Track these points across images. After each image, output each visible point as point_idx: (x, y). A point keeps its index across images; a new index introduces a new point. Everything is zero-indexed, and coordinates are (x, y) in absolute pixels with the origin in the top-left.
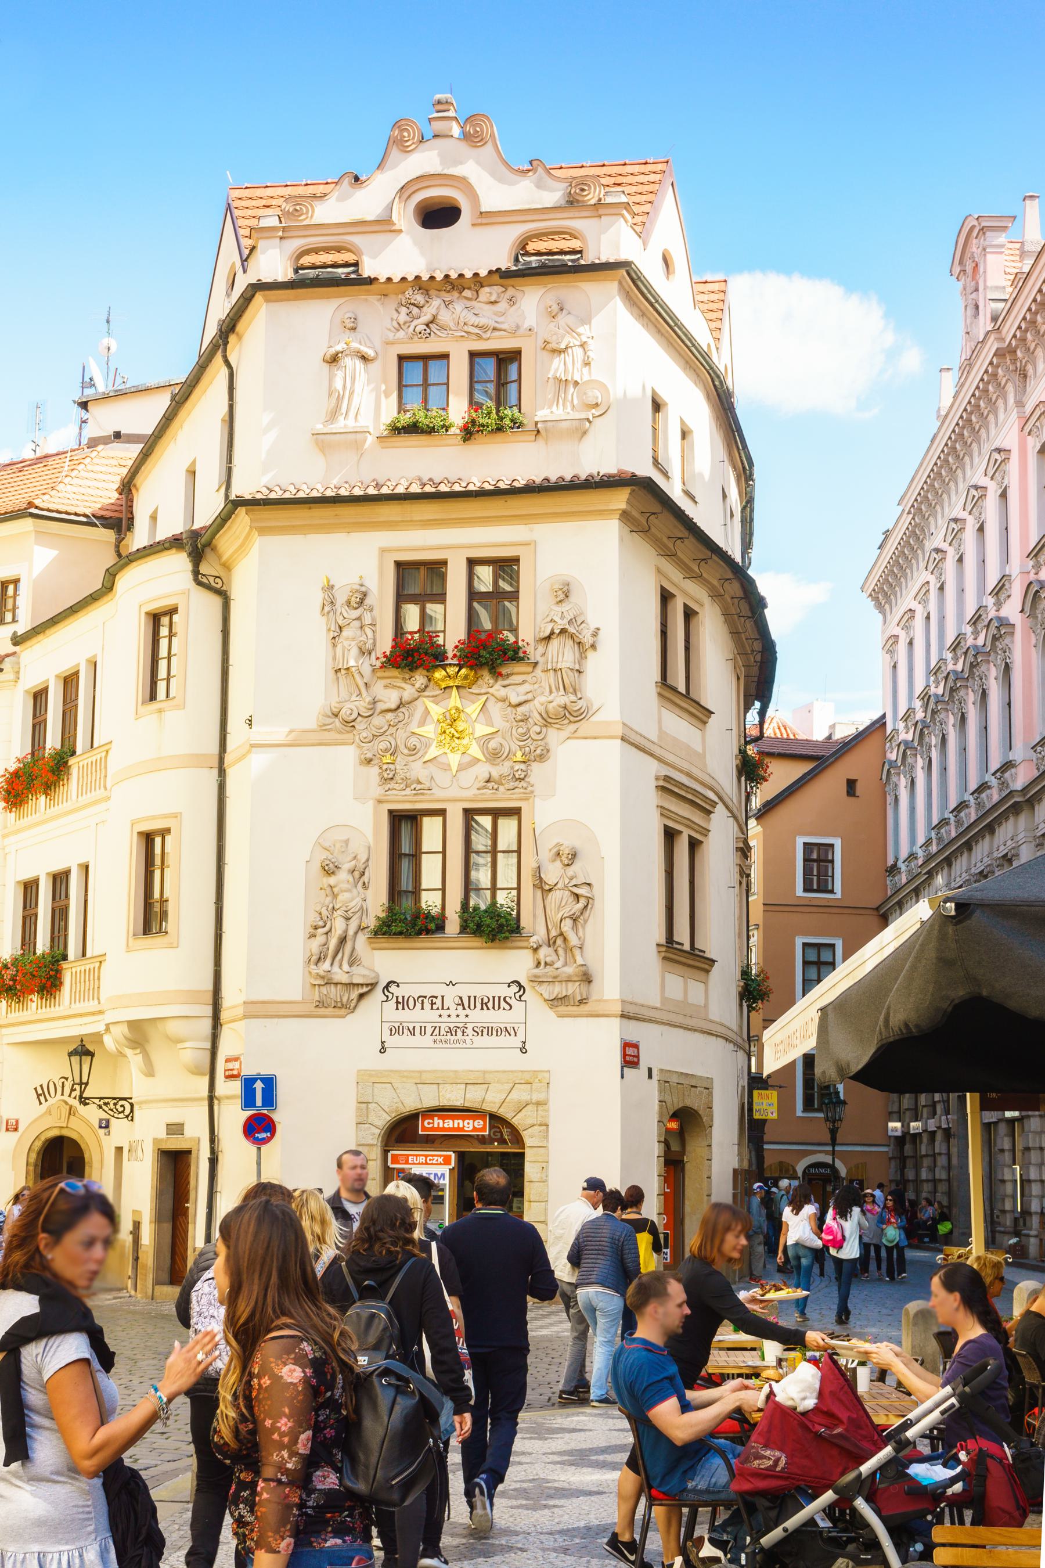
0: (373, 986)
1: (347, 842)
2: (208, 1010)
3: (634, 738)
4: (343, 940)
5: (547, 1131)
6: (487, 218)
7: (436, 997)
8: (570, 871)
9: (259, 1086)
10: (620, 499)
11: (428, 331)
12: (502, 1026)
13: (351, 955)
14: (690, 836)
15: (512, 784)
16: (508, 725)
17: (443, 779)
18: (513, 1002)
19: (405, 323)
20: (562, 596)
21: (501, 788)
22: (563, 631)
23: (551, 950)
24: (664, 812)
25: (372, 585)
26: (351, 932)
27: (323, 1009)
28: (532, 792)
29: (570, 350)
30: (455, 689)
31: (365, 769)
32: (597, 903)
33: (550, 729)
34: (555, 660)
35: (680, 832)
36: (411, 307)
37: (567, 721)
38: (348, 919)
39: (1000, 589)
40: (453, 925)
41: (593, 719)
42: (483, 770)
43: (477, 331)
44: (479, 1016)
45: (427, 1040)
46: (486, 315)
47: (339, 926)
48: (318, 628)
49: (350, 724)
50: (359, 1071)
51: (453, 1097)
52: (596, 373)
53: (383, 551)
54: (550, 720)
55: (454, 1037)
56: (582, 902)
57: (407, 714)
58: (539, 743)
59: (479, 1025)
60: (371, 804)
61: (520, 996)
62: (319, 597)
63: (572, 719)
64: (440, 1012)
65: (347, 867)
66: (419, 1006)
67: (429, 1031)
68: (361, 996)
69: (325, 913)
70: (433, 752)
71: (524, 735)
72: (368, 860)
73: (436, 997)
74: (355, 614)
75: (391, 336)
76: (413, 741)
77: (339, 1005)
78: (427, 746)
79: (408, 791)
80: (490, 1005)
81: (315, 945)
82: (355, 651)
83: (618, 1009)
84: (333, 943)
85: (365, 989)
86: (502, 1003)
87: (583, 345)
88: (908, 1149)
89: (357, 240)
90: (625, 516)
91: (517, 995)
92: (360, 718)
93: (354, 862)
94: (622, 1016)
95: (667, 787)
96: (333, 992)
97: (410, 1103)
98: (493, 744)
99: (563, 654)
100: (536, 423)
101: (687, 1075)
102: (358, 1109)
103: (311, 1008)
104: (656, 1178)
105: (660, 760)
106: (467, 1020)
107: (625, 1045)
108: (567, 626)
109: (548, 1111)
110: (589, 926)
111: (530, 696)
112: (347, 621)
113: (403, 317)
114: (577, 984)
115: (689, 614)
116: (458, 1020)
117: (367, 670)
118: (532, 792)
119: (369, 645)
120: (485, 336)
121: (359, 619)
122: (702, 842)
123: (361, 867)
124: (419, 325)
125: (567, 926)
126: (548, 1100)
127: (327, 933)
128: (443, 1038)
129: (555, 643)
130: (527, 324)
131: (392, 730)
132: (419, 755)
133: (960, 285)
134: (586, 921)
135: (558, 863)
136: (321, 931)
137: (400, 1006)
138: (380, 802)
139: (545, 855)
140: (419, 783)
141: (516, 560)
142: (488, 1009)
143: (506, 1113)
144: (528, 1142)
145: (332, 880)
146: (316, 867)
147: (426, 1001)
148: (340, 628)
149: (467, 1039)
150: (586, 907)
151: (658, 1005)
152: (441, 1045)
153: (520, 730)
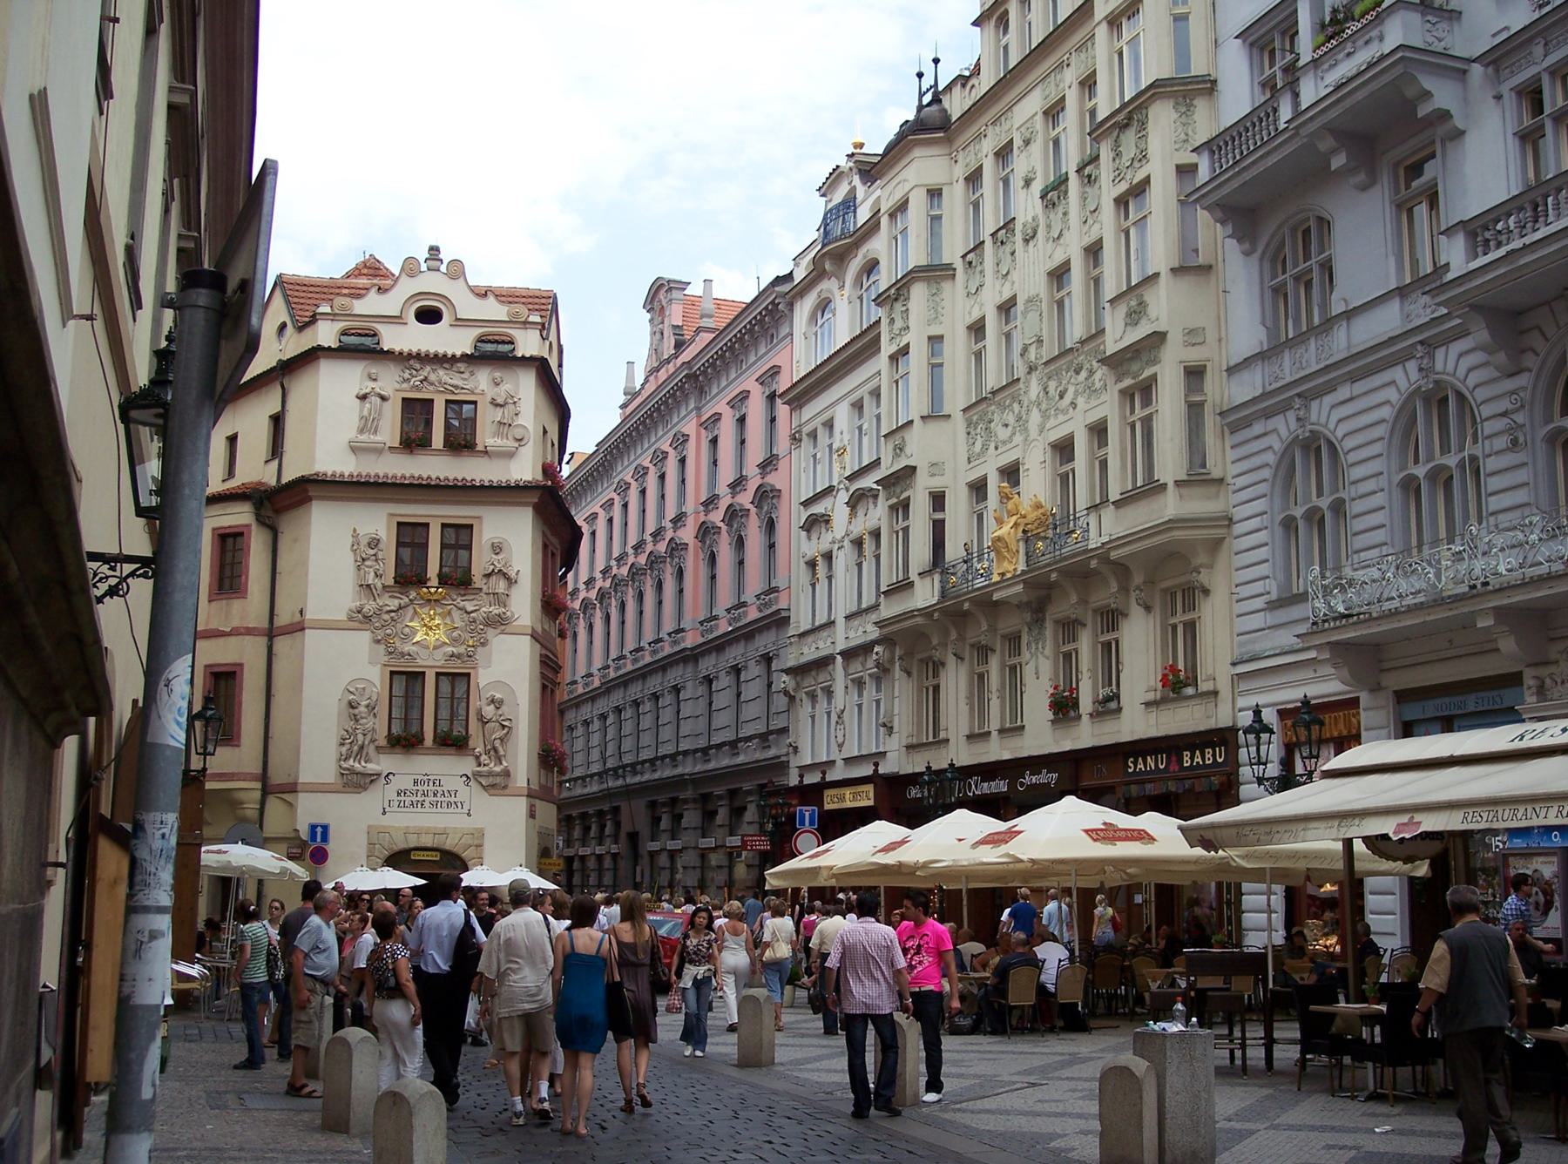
2: (258, 785)
4: (362, 747)
6: (460, 322)
8: (500, 712)
17: (424, 653)
22: (500, 571)
24: (543, 676)
25: (383, 535)
31: (377, 646)
39: (679, 520)
42: (450, 649)
48: (349, 560)
51: (427, 841)
52: (520, 420)
62: (350, 540)
65: (364, 703)
68: (372, 781)
70: (417, 638)
74: (372, 552)
76: (407, 630)
81: (344, 750)
82: (372, 574)
84: (356, 748)
88: (576, 865)
94: (529, 796)
97: (402, 845)
98: (455, 634)
115: (553, 554)
117: (379, 586)
123: (372, 704)
124: (415, 381)
129: (494, 578)
130: (481, 388)
133: (648, 316)
139: (484, 701)
141: (471, 527)
145: (356, 711)
146: (345, 702)
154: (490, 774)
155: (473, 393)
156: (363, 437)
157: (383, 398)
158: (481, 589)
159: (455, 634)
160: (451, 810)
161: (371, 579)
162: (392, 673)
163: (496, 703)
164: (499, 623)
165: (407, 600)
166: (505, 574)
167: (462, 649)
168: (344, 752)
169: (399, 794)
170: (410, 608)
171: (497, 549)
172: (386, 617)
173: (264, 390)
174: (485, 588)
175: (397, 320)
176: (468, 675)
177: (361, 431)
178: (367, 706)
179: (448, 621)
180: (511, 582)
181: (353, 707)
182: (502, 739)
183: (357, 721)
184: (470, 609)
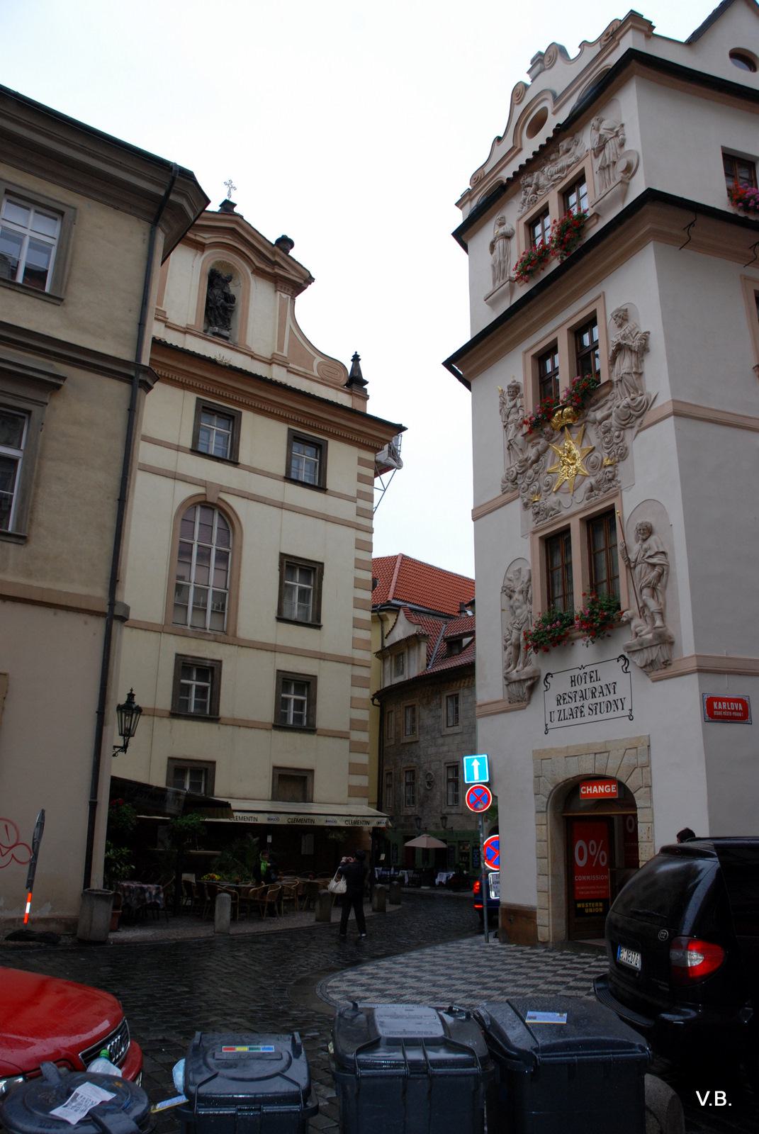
1: (519, 571)
3: (701, 413)
5: (651, 792)
8: (645, 546)
10: (647, 223)
16: (599, 440)
17: (566, 500)
19: (525, 200)
20: (620, 321)
21: (601, 493)
25: (520, 379)
27: (514, 704)
28: (620, 487)
29: (607, 144)
30: (566, 428)
32: (671, 569)
37: (634, 418)
41: (652, 408)
43: (558, 175)
46: (564, 161)
51: (587, 766)
53: (525, 352)
54: (624, 423)
56: (657, 569)
57: (543, 460)
61: (626, 668)
62: (498, 400)
63: (637, 413)
68: (532, 689)
71: (608, 443)
72: (530, 580)
76: (548, 478)
77: (519, 699)
78: (555, 480)
79: (549, 519)
83: (693, 665)
85: (529, 683)
90: (660, 236)
91: (624, 668)
92: (519, 476)
94: (700, 671)
96: (514, 687)
103: (506, 704)
111: (610, 411)
113: (523, 196)
114: (659, 646)
117: (519, 437)
118: (620, 487)
120: (563, 175)
121: (515, 406)
123: (524, 586)
126: (649, 761)
134: (665, 587)
135: (640, 542)
140: (554, 509)
144: (639, 803)
150: (660, 575)
153: (607, 440)
156: (497, 285)
158: (610, 383)
159: (592, 459)
160: (611, 714)
163: (646, 532)
164: (636, 415)
166: (630, 349)
167: (600, 475)
169: (559, 703)
170: (550, 452)
171: (622, 317)
173: (264, 280)
174: (615, 379)
175: (515, 150)
178: (522, 592)
179: (585, 446)
181: (510, 597)
182: (654, 589)
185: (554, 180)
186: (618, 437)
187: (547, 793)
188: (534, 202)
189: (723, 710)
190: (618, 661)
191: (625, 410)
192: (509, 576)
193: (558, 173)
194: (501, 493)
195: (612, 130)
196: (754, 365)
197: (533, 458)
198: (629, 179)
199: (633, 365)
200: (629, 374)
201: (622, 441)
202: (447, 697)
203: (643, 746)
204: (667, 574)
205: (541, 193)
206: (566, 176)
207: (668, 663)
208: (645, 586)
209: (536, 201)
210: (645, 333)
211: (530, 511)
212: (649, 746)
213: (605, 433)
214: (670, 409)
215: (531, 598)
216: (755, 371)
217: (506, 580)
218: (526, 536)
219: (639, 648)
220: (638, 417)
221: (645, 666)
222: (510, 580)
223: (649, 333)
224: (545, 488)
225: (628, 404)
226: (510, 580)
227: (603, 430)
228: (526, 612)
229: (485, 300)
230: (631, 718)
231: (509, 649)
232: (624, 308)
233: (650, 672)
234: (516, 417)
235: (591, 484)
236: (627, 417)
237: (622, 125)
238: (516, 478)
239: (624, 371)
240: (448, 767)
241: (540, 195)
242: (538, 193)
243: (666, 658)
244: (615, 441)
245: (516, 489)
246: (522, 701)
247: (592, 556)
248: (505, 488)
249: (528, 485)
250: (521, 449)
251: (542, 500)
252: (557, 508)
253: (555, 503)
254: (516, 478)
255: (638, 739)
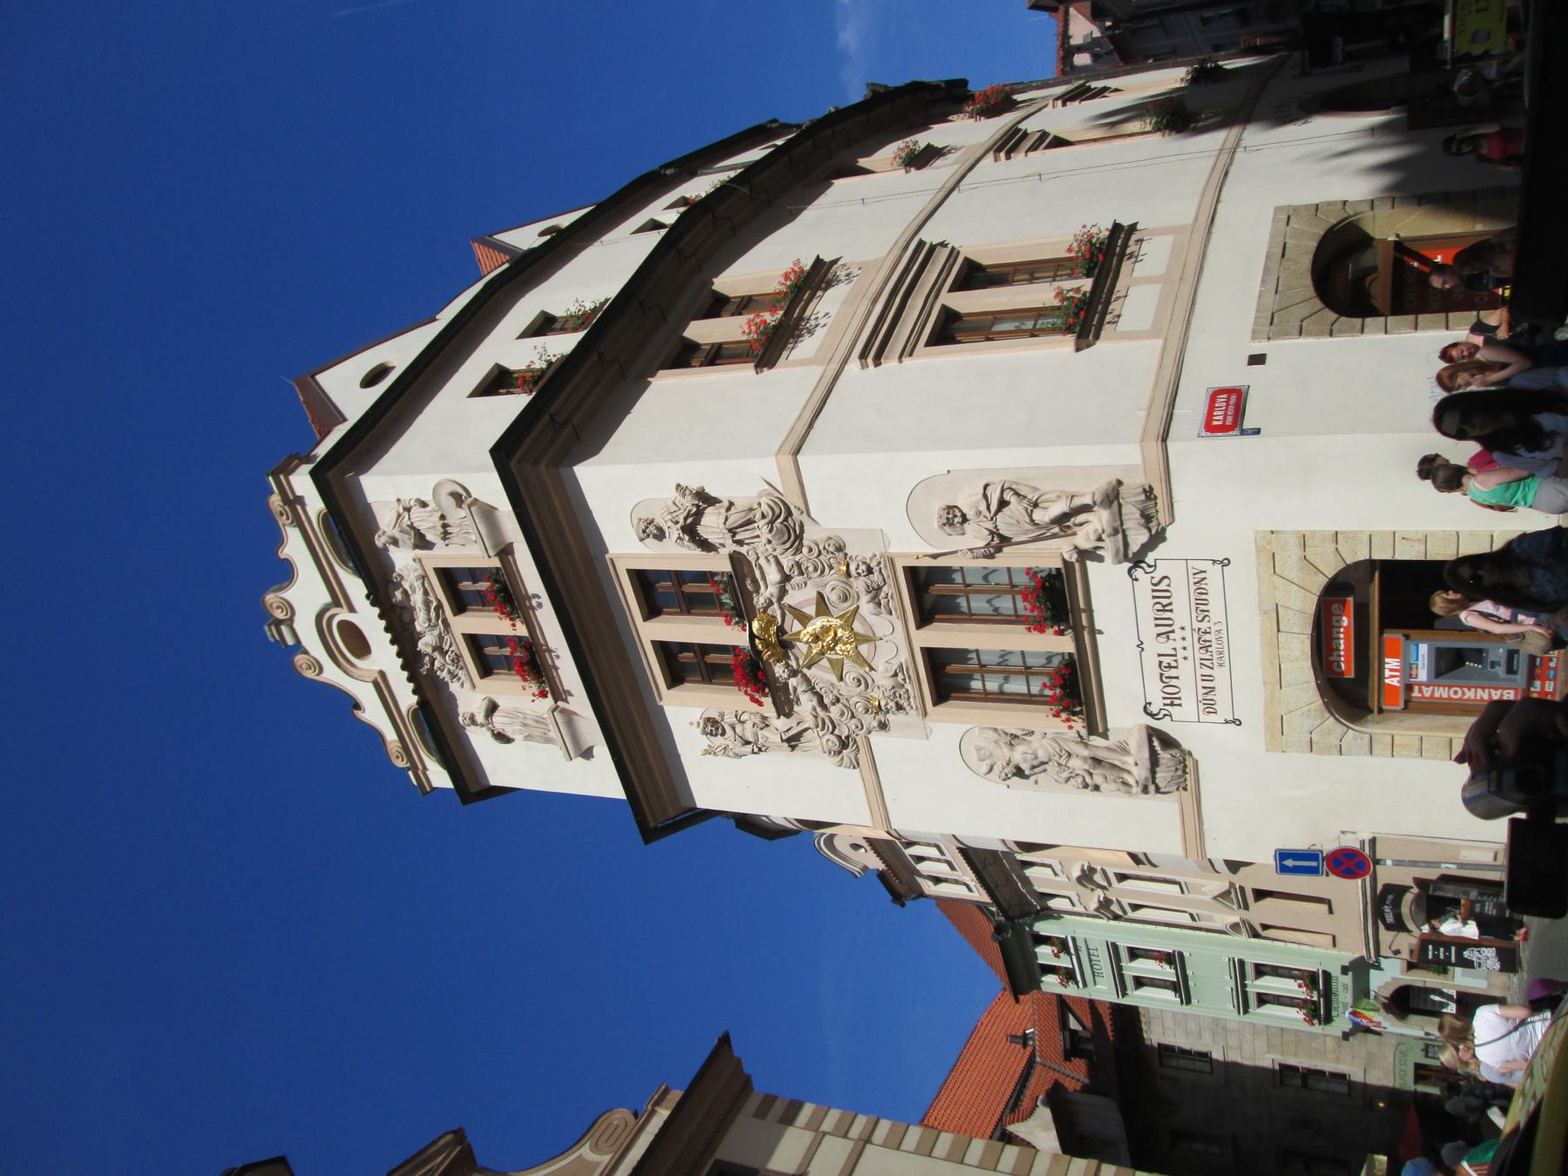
0: (1152, 733)
3: (801, 429)
5: (1344, 533)
6: (339, 597)
7: (1161, 663)
8: (970, 514)
9: (1289, 863)
11: (450, 653)
12: (1193, 588)
13: (1115, 751)
14: (951, 290)
15: (876, 577)
18: (1158, 575)
21: (885, 589)
22: (686, 529)
23: (1081, 532)
24: (908, 351)
26: (1086, 753)
32: (1009, 477)
33: (805, 536)
34: (721, 536)
35: (944, 308)
36: (435, 668)
38: (1070, 755)
40: (1066, 644)
41: (781, 491)
44: (1182, 613)
45: (1220, 675)
46: (417, 599)
47: (1076, 764)
49: (844, 744)
50: (1267, 750)
51: (1299, 646)
55: (1214, 643)
56: (1008, 496)
58: (821, 547)
59: (1194, 614)
60: (928, 723)
61: (1149, 566)
62: (721, 760)
64: (1179, 657)
65: (1006, 750)
66: (1173, 682)
67: (1207, 671)
68: (1168, 742)
69: (1066, 775)
71: (816, 569)
73: (1161, 663)
75: (467, 685)
77: (1181, 766)
79: (908, 686)
80: (1165, 602)
82: (765, 732)
83: (1154, 447)
85: (1156, 743)
86: (1160, 587)
87: (408, 510)
89: (404, 710)
91: (1148, 570)
92: (836, 732)
93: (1003, 746)
95: (875, 350)
96: (1162, 776)
99: (711, 528)
100: (490, 557)
101: (1266, 270)
102: (1320, 752)
104: (1420, 334)
105: (845, 361)
106: (1188, 628)
107: (1210, 428)
108: (679, 526)
109: (1313, 532)
110: (1044, 486)
111: (772, 560)
112: (738, 739)
114: (1121, 501)
116: (1189, 638)
117: (781, 723)
118: (882, 556)
119: (757, 720)
120: (435, 604)
122: (967, 261)
125: (1041, 516)
127: (1091, 774)
128: (1215, 656)
130: (412, 562)
131: (843, 700)
132: (864, 674)
134: (1035, 489)
136: (1088, 780)
137: (1176, 702)
138: (925, 714)
140: (896, 675)
142: (1170, 604)
143: (1319, 583)
144: (1363, 556)
147: (1166, 674)
148: (748, 743)
149: (1214, 628)
151: (1160, 342)
152: (1226, 659)
154: (1119, 530)
155: (424, 577)
156: (554, 734)
157: (492, 708)
158: (736, 559)
161: (772, 736)
162: (940, 696)
163: (954, 518)
165: (793, 682)
167: (859, 585)
168: (1113, 786)
172: (835, 711)
176: (912, 572)
177: (548, 740)
179: (810, 610)
180: (705, 499)
182: (1036, 505)
183: (1043, 763)
184: (773, 576)
185: (437, 617)
186: (811, 550)
187: (1340, 729)
188: (458, 659)
189: (1225, 415)
190: (1136, 580)
191: (775, 529)
192: (985, 769)
193: (428, 610)
194: (857, 770)
195: (399, 515)
196: (754, 372)
197: (815, 702)
198: (470, 496)
199: (716, 511)
200: (726, 519)
201: (818, 546)
202: (1161, 1064)
203: (1271, 542)
204: (1016, 483)
205: (448, 643)
206: (437, 598)
207: (1148, 489)
208: (1031, 517)
209: (456, 654)
210: (677, 488)
211: (890, 716)
212: (1272, 532)
213: (801, 573)
214: (787, 460)
215: (1023, 730)
216: (762, 372)
217: (989, 776)
218: (928, 730)
219: (1120, 536)
220: (789, 513)
221: (1150, 530)
222: (991, 769)
223: (678, 486)
224: (863, 686)
225: (768, 524)
226: (991, 769)
227: (796, 572)
228: (1044, 741)
229: (571, 759)
230: (1226, 562)
231: (1098, 779)
232: (635, 521)
233: (1159, 524)
234: (748, 725)
235: (869, 602)
236: (785, 529)
237: (399, 500)
238: (839, 737)
239: (722, 526)
240: (1282, 1083)
241: (450, 646)
242: (446, 648)
243: (1140, 490)
244: (816, 555)
245: (855, 742)
246: (1185, 766)
247: (974, 617)
248: (851, 761)
249: (853, 716)
250: (798, 723)
251: (877, 694)
252: (896, 667)
253: (887, 670)
254: (839, 737)
255: (1259, 550)
